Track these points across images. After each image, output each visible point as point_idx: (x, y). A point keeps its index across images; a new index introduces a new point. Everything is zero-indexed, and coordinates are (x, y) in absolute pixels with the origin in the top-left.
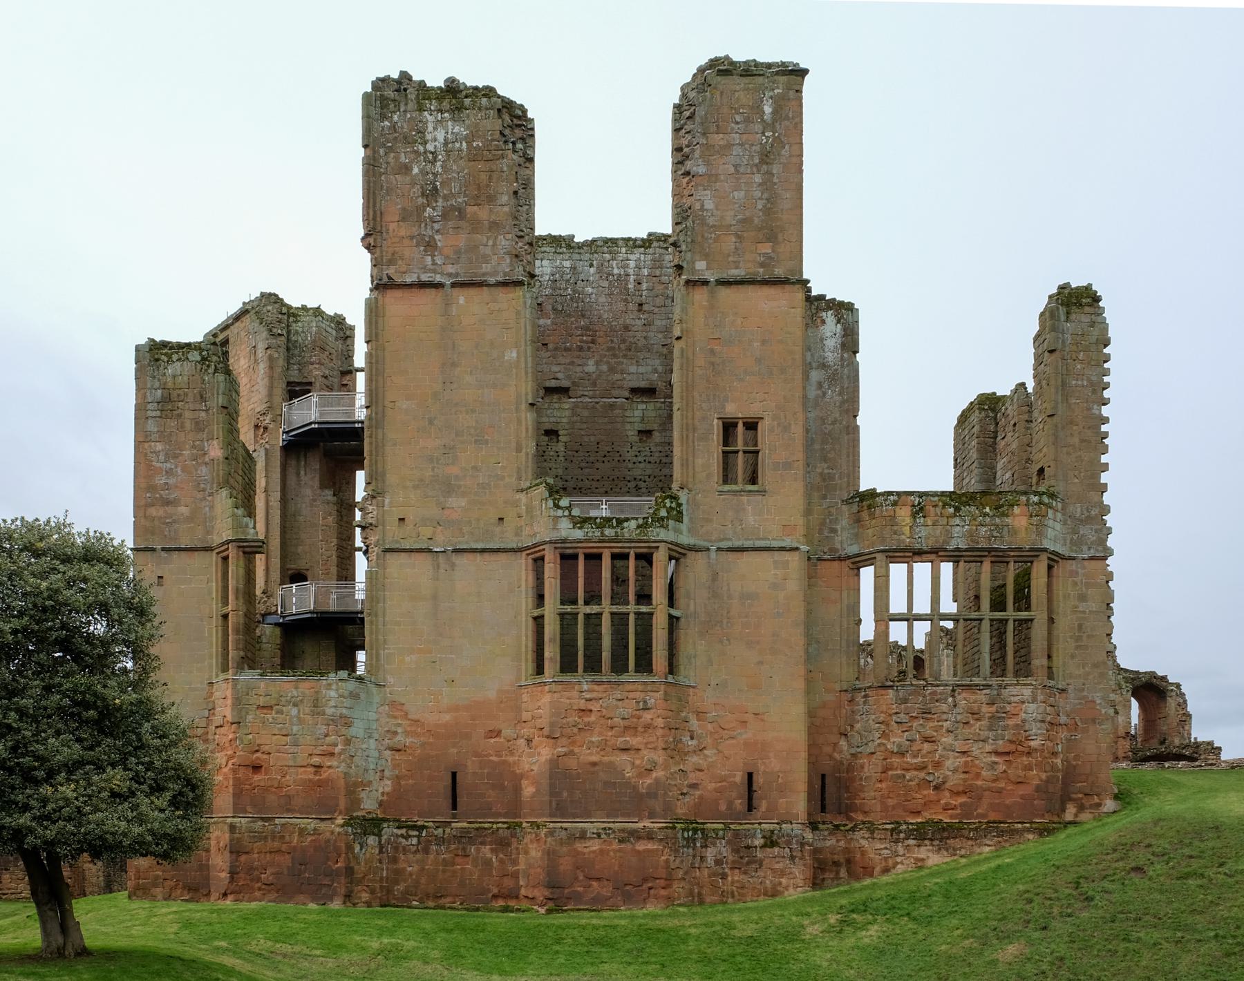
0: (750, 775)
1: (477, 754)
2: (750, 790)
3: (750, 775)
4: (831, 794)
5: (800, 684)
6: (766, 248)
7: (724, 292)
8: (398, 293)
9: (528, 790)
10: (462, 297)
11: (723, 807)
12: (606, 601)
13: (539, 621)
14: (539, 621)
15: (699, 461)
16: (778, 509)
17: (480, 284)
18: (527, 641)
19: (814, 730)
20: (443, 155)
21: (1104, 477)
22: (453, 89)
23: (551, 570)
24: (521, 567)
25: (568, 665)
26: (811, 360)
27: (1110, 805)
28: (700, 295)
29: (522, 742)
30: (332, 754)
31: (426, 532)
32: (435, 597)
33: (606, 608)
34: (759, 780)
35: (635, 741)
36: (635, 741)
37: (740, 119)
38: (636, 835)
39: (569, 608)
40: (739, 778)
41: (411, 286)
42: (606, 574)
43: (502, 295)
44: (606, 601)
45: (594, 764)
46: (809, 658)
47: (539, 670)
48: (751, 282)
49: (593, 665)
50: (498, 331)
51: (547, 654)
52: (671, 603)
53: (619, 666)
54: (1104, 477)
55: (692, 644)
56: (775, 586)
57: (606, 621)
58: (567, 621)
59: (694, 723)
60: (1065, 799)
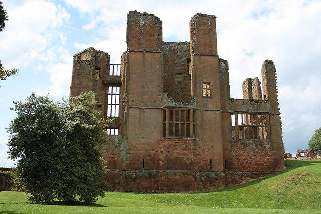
0: (211, 160)
1: (149, 155)
2: (211, 162)
3: (211, 160)
4: (228, 165)
5: (221, 140)
6: (210, 49)
7: (202, 57)
8: (133, 53)
9: (161, 163)
10: (147, 55)
11: (205, 168)
12: (179, 120)
13: (164, 124)
14: (164, 124)
15: (198, 91)
16: (215, 104)
17: (151, 52)
18: (161, 129)
19: (224, 150)
20: (143, 28)
21: (278, 98)
22: (145, 14)
23: (167, 113)
24: (159, 113)
25: (171, 134)
26: (220, 71)
27: (285, 168)
28: (197, 57)
29: (160, 152)
30: (116, 154)
31: (138, 103)
32: (140, 118)
33: (179, 122)
34: (212, 161)
35: (187, 152)
36: (187, 152)
37: (204, 26)
38: (187, 174)
39: (171, 122)
40: (209, 161)
41: (137, 51)
42: (179, 114)
43: (156, 54)
44: (179, 120)
45: (177, 158)
46: (222, 133)
47: (164, 135)
48: (208, 55)
49: (176, 135)
50: (155, 61)
51: (166, 132)
52: (194, 122)
53: (182, 135)
54: (278, 98)
55: (199, 131)
56: (215, 118)
57: (179, 126)
58: (171, 124)
59: (198, 149)
60: (276, 166)
